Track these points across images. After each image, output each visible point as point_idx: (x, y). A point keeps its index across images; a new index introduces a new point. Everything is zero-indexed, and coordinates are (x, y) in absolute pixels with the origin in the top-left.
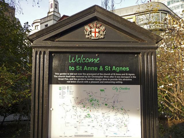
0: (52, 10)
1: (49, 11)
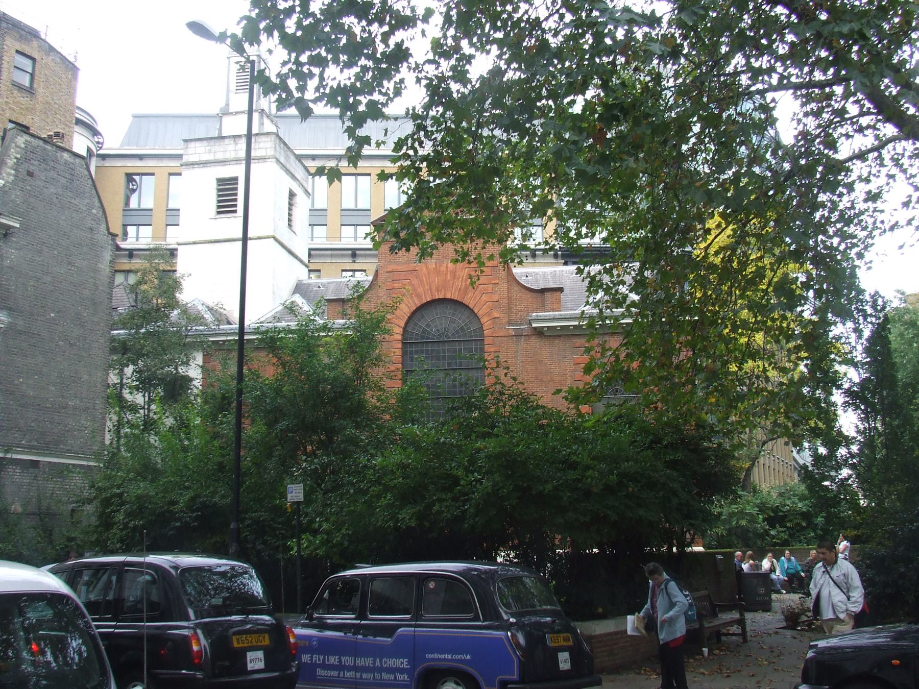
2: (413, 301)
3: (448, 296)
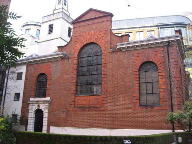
0: (60, 6)
1: (55, 8)
2: (81, 44)
3: (92, 42)
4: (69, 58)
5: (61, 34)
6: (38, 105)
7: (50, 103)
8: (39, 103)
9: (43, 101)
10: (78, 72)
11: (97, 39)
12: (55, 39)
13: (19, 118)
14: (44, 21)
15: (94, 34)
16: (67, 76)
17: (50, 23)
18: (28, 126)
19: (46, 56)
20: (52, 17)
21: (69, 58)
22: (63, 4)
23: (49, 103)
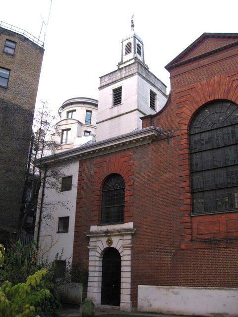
0: (131, 56)
1: (122, 61)
3: (217, 97)
4: (168, 138)
5: (138, 104)
6: (108, 240)
7: (134, 234)
8: (111, 235)
9: (119, 231)
10: (191, 165)
11: (229, 89)
12: (127, 113)
13: (69, 267)
14: (103, 84)
15: (219, 82)
16: (167, 175)
17: (116, 86)
18: (89, 284)
19: (119, 139)
20: (118, 75)
21: (168, 138)
22: (135, 51)
23: (132, 235)
